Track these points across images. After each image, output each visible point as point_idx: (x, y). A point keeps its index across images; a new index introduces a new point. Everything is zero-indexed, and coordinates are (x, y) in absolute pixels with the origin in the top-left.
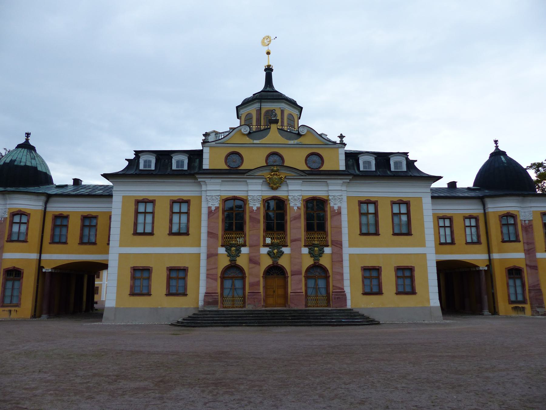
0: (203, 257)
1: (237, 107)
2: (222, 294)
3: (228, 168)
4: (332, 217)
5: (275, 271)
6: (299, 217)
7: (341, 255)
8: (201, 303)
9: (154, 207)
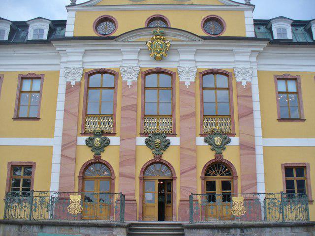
0: (57, 151)
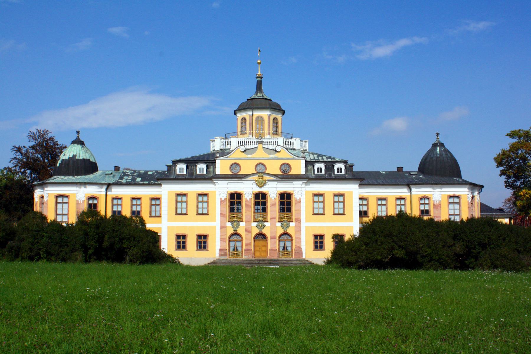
1: (235, 111)
2: (229, 250)
3: (231, 173)
4: (295, 204)
5: (261, 236)
6: (275, 204)
7: (300, 227)
9: (187, 198)
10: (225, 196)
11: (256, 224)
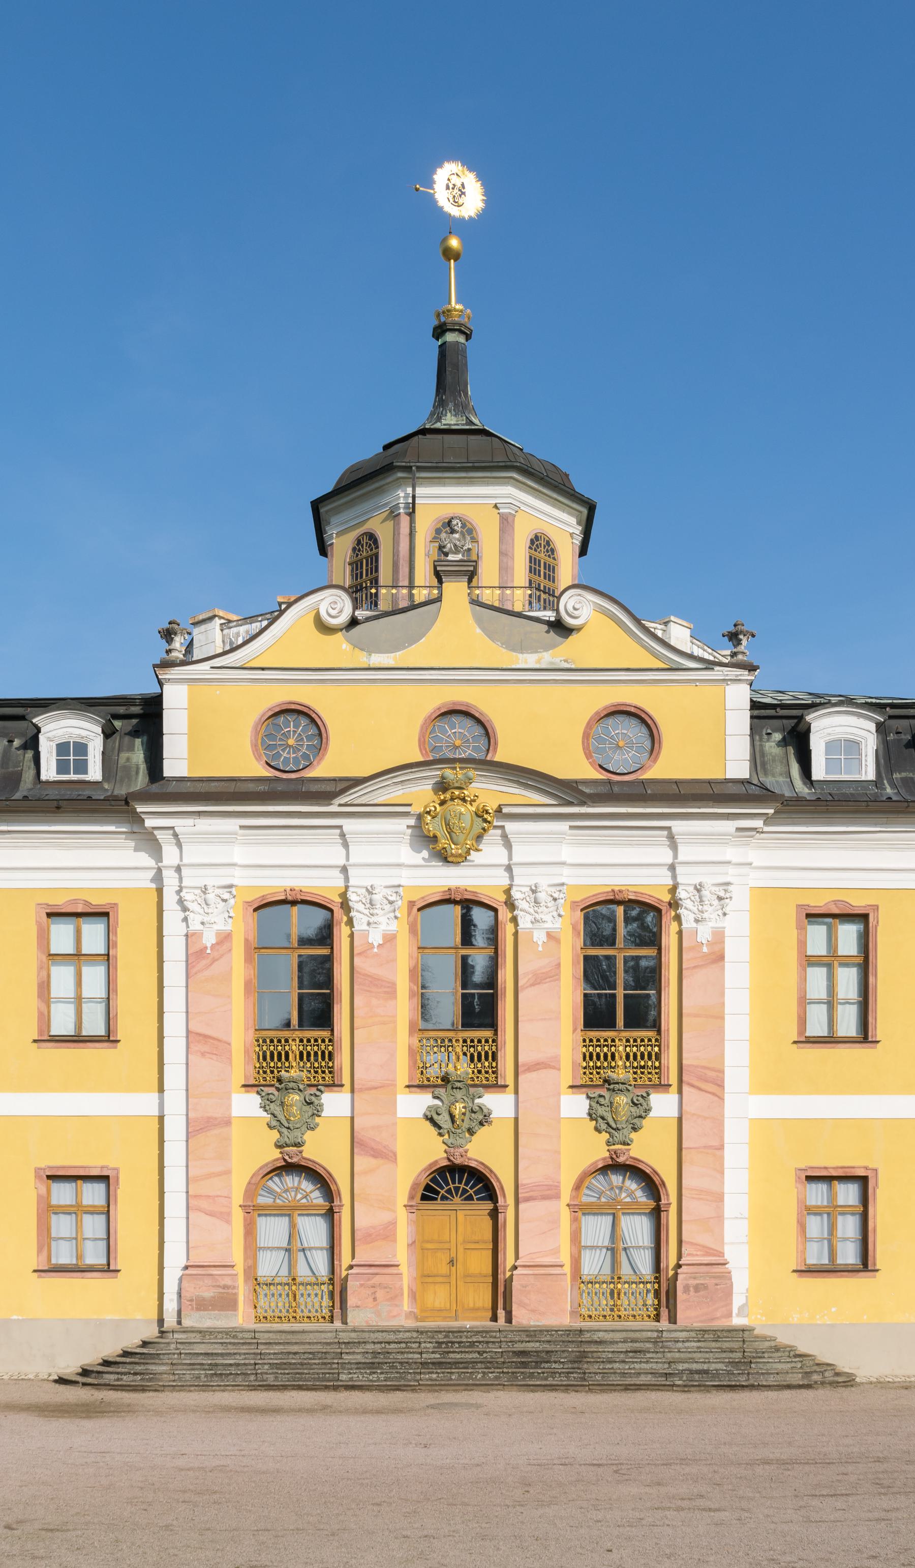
0: (175, 1130)
5: (457, 1182)
6: (552, 975)
8: (170, 1305)
10: (222, 921)
11: (424, 1101)
